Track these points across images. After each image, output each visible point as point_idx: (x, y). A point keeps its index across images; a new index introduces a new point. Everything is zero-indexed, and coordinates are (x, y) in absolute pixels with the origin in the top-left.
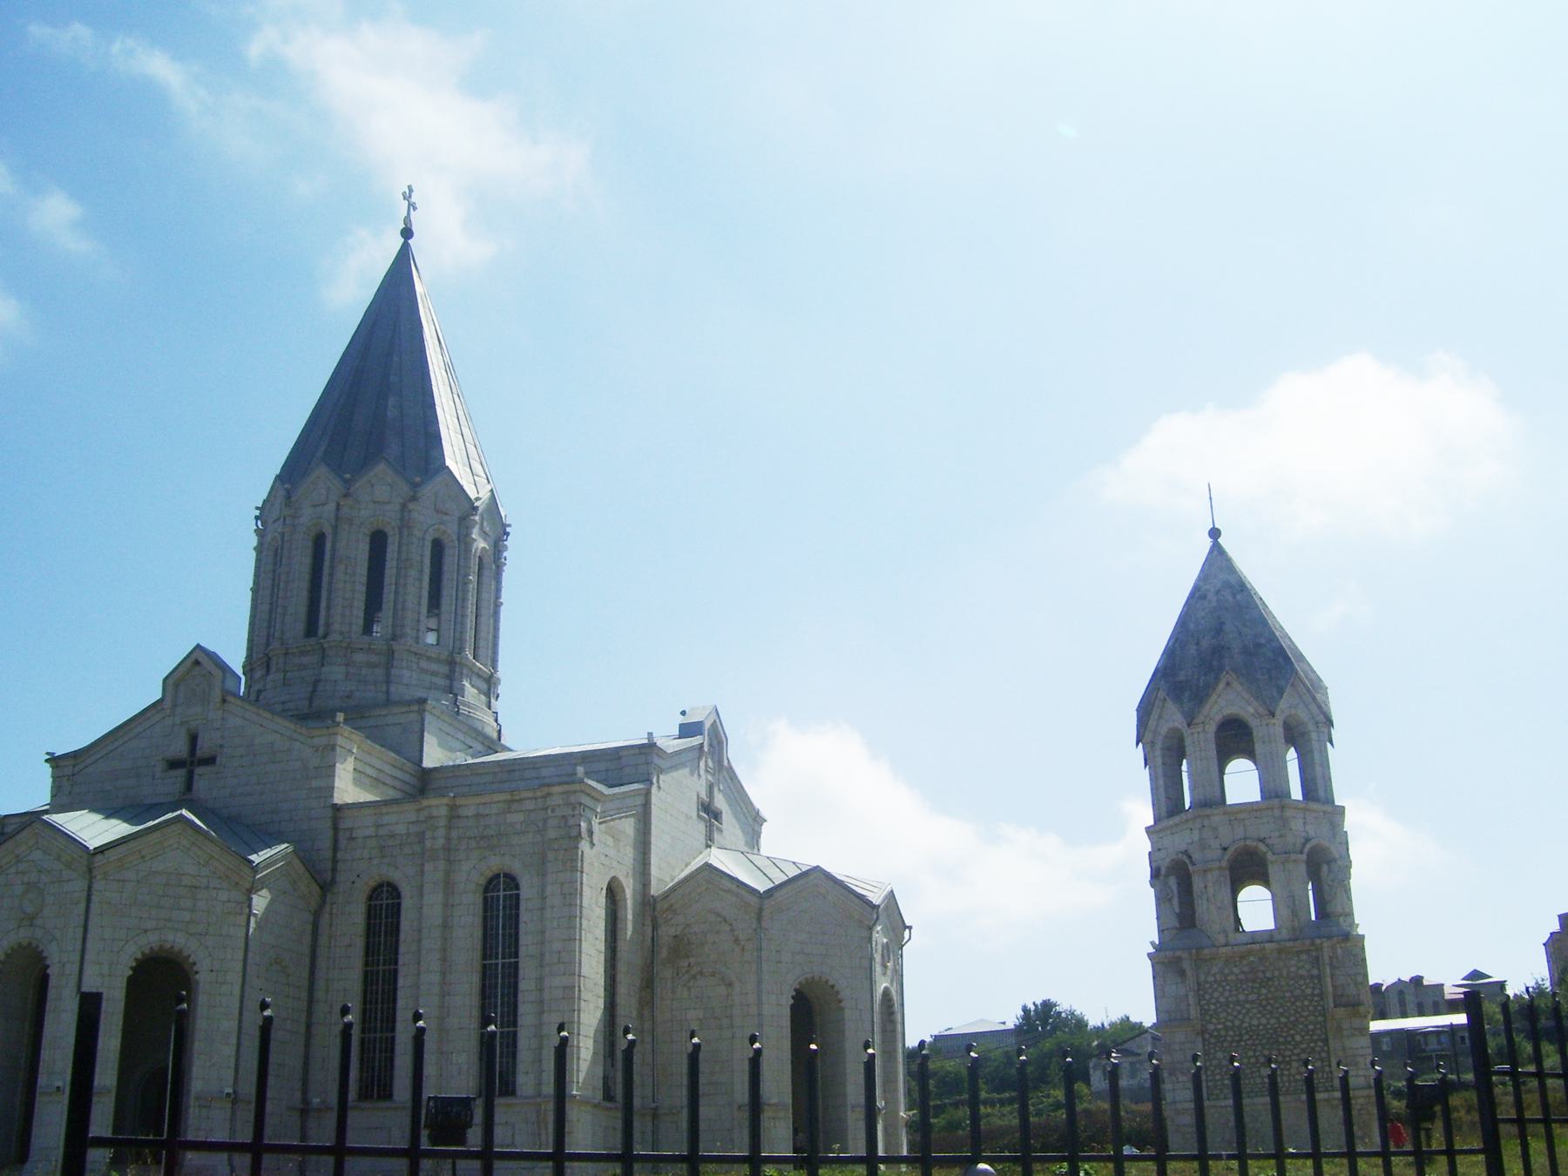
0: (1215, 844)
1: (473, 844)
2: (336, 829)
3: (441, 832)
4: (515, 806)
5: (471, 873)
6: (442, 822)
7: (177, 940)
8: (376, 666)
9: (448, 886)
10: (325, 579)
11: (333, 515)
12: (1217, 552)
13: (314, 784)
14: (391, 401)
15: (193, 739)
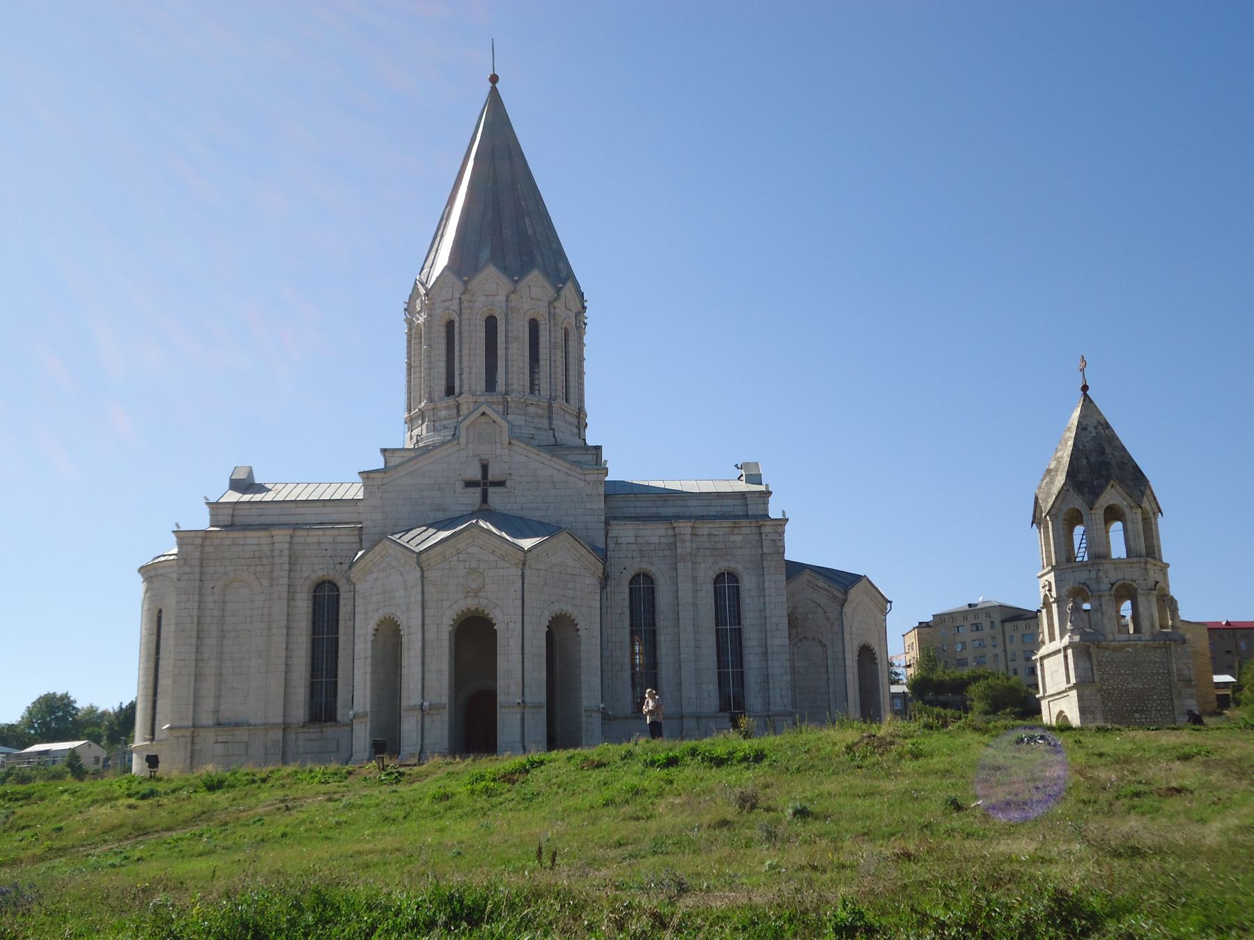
0: (1106, 580)
1: (708, 553)
2: (606, 537)
3: (688, 544)
4: (736, 531)
5: (707, 571)
6: (688, 537)
7: (568, 609)
8: (541, 417)
9: (694, 579)
10: (501, 352)
11: (504, 304)
12: (1087, 401)
13: (588, 506)
14: (527, 220)
15: (485, 468)
